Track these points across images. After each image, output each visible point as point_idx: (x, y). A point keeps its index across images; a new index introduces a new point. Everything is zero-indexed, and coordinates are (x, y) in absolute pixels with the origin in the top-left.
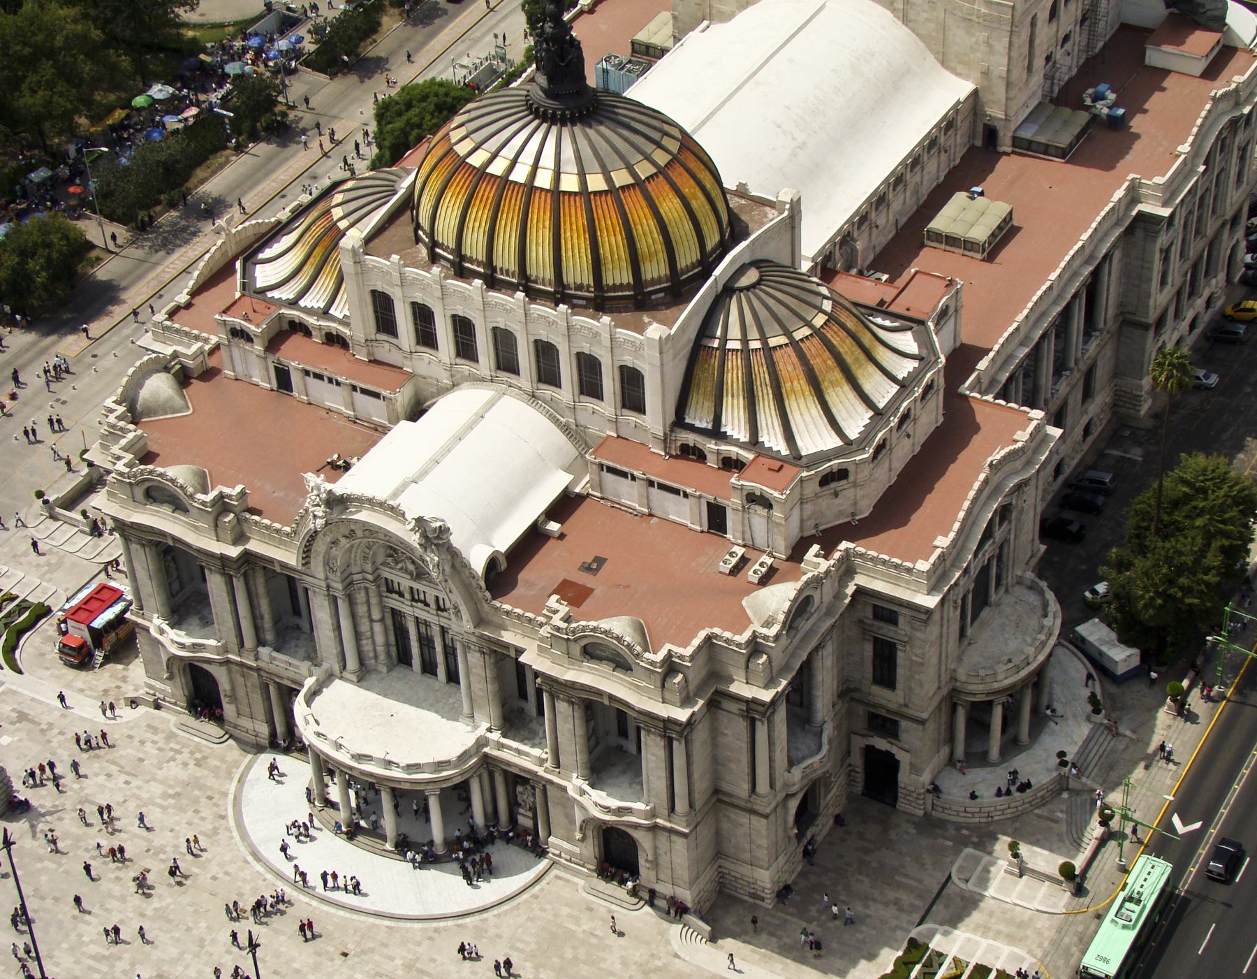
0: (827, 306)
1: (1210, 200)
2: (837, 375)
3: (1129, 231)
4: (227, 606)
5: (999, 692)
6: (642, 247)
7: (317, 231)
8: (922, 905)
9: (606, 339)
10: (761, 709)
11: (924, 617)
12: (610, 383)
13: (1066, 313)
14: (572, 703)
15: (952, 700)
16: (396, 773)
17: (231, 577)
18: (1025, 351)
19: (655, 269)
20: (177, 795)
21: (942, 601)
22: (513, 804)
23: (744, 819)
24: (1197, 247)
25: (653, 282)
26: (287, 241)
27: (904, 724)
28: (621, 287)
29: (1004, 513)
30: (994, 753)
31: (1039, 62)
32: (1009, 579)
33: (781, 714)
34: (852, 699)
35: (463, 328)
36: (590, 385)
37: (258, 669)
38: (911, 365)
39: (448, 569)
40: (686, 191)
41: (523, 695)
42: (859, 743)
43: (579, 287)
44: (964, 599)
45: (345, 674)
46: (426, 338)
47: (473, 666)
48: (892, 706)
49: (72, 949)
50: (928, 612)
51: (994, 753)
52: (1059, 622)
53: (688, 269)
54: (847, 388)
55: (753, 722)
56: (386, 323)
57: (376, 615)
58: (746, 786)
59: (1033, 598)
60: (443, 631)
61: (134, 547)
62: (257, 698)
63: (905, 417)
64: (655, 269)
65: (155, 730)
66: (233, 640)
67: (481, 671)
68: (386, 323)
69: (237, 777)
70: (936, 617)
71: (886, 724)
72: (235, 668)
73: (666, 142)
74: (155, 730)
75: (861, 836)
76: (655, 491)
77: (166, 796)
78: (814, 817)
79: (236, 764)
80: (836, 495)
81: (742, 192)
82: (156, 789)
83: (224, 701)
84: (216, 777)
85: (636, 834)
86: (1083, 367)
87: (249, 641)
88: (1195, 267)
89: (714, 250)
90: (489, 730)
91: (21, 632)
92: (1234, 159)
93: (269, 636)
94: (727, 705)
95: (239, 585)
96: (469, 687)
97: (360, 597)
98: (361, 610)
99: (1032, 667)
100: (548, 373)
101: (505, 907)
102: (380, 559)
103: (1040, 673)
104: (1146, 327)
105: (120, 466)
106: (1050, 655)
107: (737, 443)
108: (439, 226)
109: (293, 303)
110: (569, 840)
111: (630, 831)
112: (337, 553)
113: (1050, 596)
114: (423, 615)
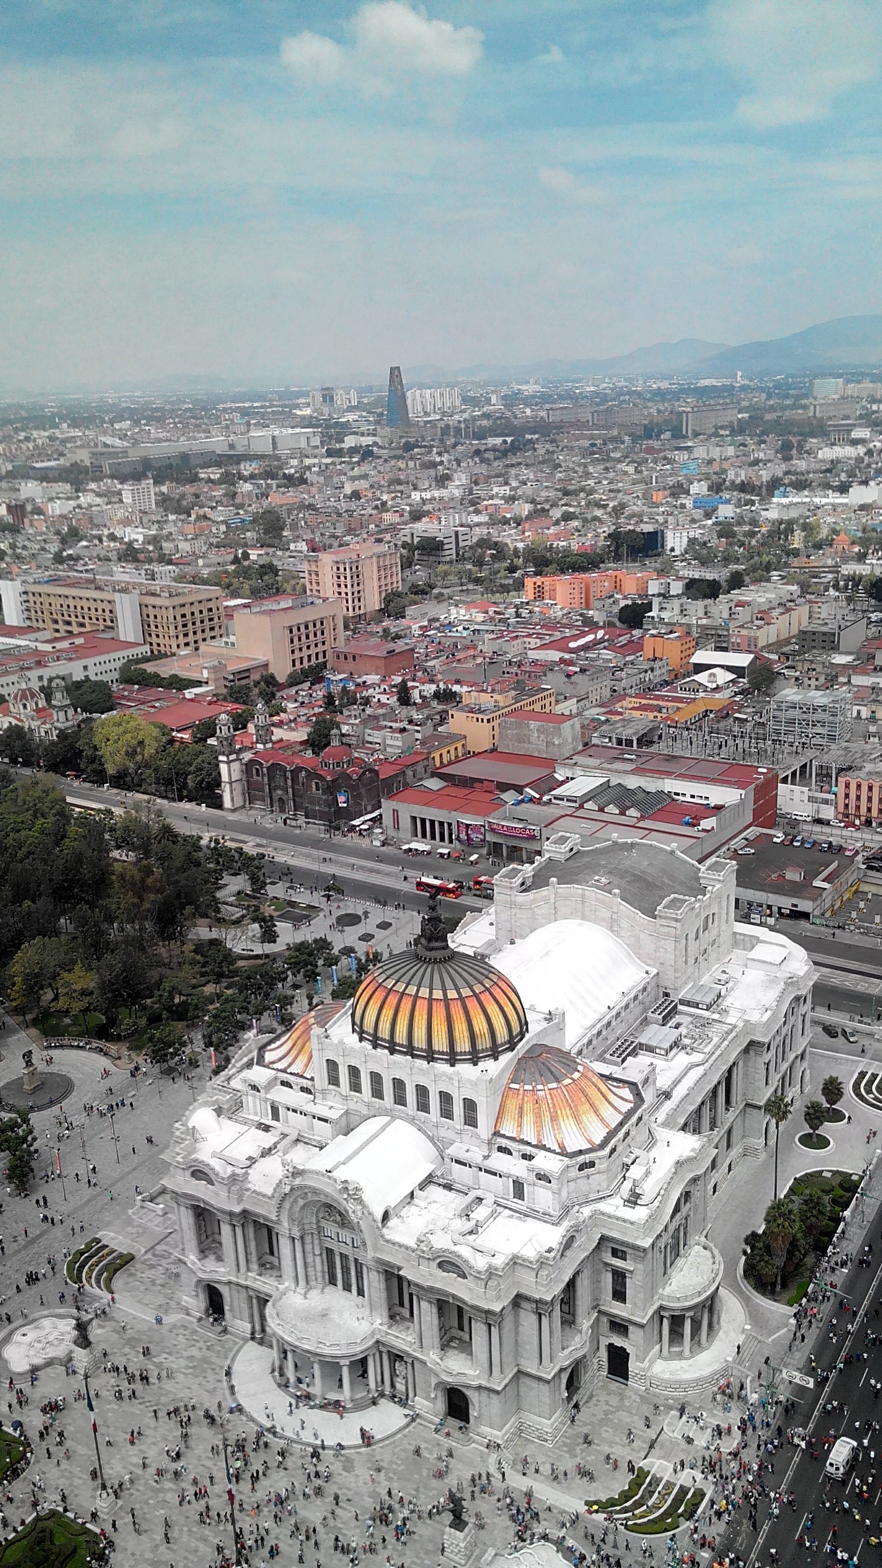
0: (580, 1068)
1: (788, 1041)
2: (588, 1106)
3: (746, 1050)
4: (232, 1246)
5: (690, 1309)
6: (476, 1029)
7: (298, 1033)
8: (647, 1446)
9: (456, 1084)
10: (546, 1307)
11: (642, 1254)
12: (458, 1109)
13: (714, 1091)
14: (430, 1302)
15: (659, 1314)
16: (326, 1351)
17: (234, 1226)
18: (692, 1108)
19: (484, 1043)
20: (194, 1367)
21: (653, 1245)
22: (393, 1374)
23: (535, 1384)
24: (785, 1066)
25: (483, 1051)
26: (283, 1039)
27: (631, 1328)
28: (465, 1053)
29: (686, 1195)
30: (687, 1352)
31: (691, 961)
32: (691, 1242)
33: (557, 1313)
34: (599, 1312)
35: (376, 1078)
36: (447, 1113)
37: (247, 1288)
38: (630, 1105)
39: (359, 1214)
40: (501, 1002)
41: (402, 1304)
42: (604, 1342)
43: (443, 1053)
44: (665, 1247)
45: (298, 1289)
46: (356, 1087)
47: (374, 1282)
48: (624, 1314)
49: (122, 1459)
50: (645, 1250)
51: (687, 1352)
52: (722, 1267)
53: (502, 1045)
54: (593, 1114)
55: (540, 1315)
56: (334, 1080)
57: (317, 1252)
58: (537, 1361)
59: (707, 1253)
60: (356, 1260)
61: (183, 1209)
62: (245, 1306)
63: (627, 1134)
64: (484, 1043)
65: (185, 1328)
66: (235, 1268)
67: (376, 1284)
68: (334, 1080)
69: (230, 1358)
70: (650, 1255)
71: (620, 1327)
72: (233, 1286)
73: (491, 975)
74: (185, 1328)
75: (607, 1403)
76: (483, 1173)
77: (187, 1367)
78: (578, 1388)
79: (231, 1350)
80: (588, 1177)
81: (533, 1008)
82: (182, 1363)
83: (226, 1308)
84: (218, 1357)
85: (468, 1393)
86: (726, 1127)
87: (243, 1268)
88: (783, 1078)
89: (517, 1036)
90: (381, 1324)
91: (116, 1271)
92: (800, 1021)
93: (255, 1266)
94: (524, 1304)
95: (239, 1230)
96: (370, 1296)
97: (308, 1239)
98: (308, 1247)
99: (708, 1293)
100: (423, 1107)
101: (387, 1442)
102: (321, 1215)
103: (713, 1297)
104: (759, 1108)
105: (179, 1159)
106: (718, 1288)
107: (529, 1144)
108: (365, 1021)
109: (284, 1071)
110: (427, 1398)
111: (464, 1390)
112: (297, 1209)
113: (716, 1252)
114: (347, 1251)
